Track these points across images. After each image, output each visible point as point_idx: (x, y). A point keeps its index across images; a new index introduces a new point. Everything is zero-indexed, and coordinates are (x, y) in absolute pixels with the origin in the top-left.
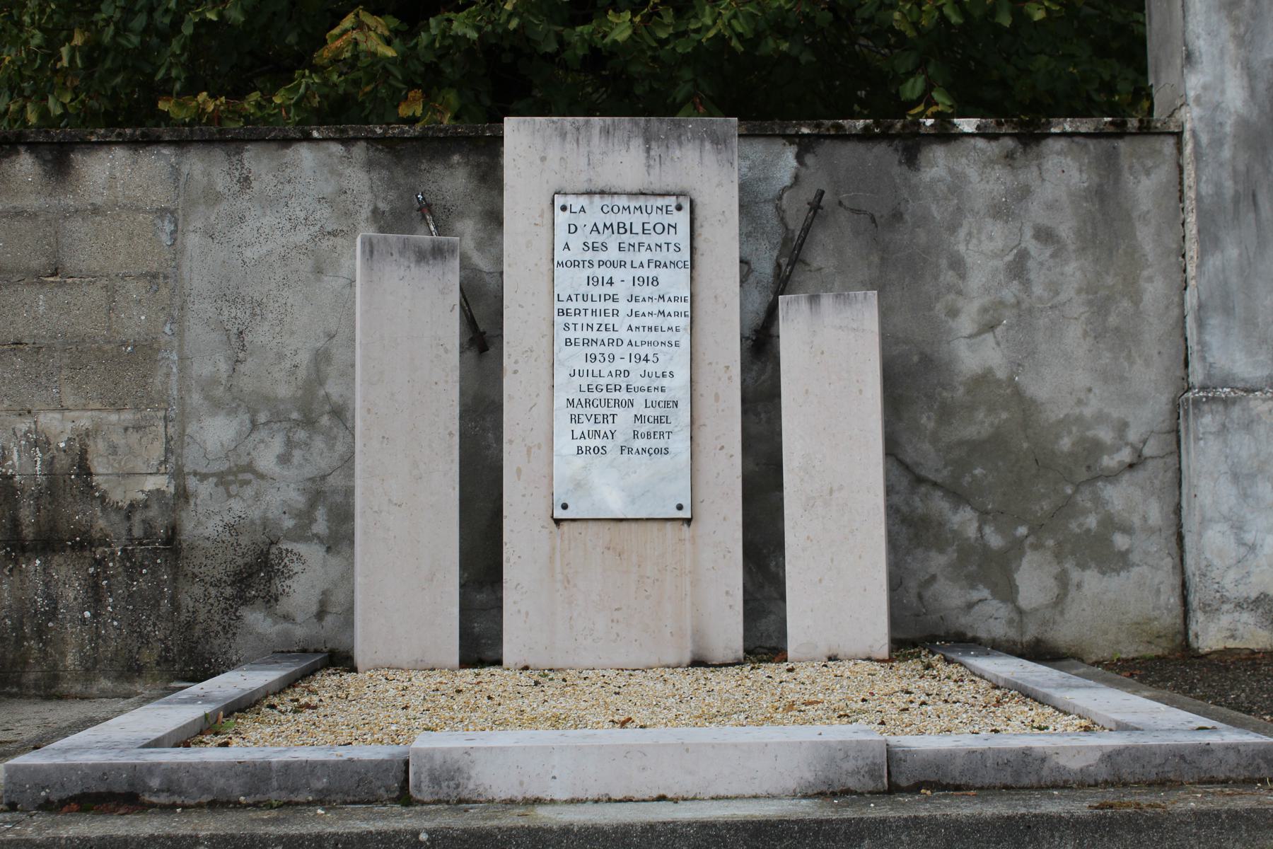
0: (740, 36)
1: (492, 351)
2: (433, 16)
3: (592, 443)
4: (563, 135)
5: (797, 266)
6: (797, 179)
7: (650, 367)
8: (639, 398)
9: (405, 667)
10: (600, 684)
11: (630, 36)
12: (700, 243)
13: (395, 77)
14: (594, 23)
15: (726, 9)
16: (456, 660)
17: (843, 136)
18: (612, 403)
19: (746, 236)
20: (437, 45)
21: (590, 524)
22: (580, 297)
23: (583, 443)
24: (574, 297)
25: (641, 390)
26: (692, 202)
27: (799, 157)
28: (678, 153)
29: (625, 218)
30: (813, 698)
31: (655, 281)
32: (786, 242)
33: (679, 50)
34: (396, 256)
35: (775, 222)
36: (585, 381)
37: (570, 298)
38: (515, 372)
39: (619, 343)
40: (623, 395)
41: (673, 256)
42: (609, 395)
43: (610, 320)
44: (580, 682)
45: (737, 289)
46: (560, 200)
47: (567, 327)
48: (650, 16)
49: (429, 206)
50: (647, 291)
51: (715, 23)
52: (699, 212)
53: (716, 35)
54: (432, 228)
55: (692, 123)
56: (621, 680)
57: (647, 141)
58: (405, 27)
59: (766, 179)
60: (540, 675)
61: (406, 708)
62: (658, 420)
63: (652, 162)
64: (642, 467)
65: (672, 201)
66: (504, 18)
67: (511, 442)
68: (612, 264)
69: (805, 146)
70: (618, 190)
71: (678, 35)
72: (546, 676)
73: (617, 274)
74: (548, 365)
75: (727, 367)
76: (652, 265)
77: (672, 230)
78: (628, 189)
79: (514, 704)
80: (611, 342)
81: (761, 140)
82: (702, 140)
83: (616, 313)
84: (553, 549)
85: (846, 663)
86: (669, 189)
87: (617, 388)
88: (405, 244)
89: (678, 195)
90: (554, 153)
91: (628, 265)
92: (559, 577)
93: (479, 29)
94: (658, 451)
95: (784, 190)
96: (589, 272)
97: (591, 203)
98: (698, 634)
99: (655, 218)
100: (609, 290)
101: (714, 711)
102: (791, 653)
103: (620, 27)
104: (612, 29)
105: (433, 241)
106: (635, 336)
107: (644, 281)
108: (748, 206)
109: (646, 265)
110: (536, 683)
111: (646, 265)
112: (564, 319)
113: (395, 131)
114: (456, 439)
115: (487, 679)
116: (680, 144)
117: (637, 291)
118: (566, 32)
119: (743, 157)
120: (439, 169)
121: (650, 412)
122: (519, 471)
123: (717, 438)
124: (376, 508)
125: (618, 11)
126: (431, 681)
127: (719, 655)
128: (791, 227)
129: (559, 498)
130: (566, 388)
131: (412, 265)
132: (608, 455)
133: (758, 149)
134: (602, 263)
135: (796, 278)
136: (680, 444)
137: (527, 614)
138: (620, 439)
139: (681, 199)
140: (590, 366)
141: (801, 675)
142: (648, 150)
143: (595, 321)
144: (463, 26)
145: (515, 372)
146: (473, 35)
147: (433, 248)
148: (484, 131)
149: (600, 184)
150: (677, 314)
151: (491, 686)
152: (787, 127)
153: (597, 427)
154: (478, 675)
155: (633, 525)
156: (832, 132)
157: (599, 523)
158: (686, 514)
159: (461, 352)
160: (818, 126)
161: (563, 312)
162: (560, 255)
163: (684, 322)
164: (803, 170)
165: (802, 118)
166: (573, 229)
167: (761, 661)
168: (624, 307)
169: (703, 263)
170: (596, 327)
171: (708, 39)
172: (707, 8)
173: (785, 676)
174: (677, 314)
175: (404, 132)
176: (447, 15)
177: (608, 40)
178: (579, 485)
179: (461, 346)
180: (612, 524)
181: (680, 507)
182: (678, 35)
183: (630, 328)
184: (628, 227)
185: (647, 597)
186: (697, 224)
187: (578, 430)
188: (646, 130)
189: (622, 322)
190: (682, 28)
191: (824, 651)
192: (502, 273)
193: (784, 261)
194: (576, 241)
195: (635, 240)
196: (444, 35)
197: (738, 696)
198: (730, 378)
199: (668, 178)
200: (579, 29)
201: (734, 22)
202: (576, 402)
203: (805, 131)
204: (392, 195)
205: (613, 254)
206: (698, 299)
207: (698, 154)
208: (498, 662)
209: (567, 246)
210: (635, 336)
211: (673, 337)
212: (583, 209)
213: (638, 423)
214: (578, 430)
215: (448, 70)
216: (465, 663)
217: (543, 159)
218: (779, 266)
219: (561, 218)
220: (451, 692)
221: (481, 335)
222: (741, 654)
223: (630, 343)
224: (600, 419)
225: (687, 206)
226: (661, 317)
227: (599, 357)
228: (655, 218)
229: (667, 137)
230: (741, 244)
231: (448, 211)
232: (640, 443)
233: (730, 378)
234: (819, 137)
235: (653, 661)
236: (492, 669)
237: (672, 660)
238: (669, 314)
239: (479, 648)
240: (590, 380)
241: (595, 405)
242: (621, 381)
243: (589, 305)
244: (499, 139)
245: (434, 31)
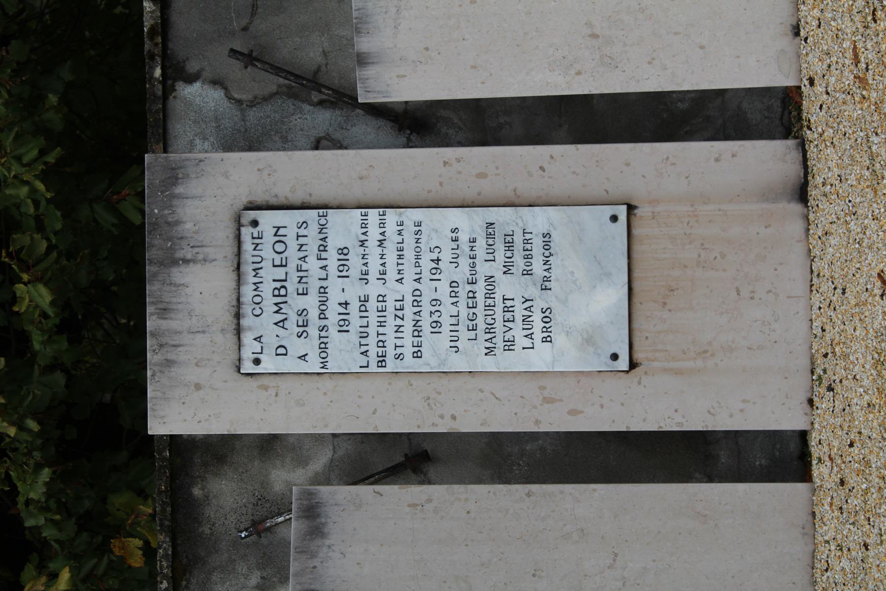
0: (43, 153)
1: (427, 446)
2: (21, 522)
4: (169, 363)
5: (322, 81)
6: (216, 82)
7: (446, 256)
8: (484, 269)
9: (811, 547)
10: (831, 313)
11: (46, 284)
12: (298, 197)
13: (95, 567)
14: (29, 328)
15: (9, 170)
16: (801, 487)
17: (164, 26)
18: (489, 301)
19: (286, 143)
20: (58, 517)
21: (635, 325)
22: (363, 341)
23: (538, 336)
24: (364, 349)
25: (473, 266)
27: (190, 79)
28: (189, 226)
29: (267, 289)
30: (849, 54)
31: (343, 251)
32: (292, 95)
33: (59, 226)
34: (316, 562)
35: (268, 108)
36: (464, 334)
37: (365, 353)
38: (454, 418)
40: (481, 288)
41: (313, 228)
43: (390, 305)
44: (828, 337)
45: (351, 152)
46: (248, 367)
47: (399, 357)
48: (20, 261)
49: (254, 524)
50: (355, 262)
51: (27, 183)
52: (260, 197)
53: (43, 181)
54: (281, 519)
55: (153, 209)
56: (826, 287)
57: (175, 262)
58: (35, 557)
59: (217, 119)
60: (819, 383)
61: (866, 546)
62: (509, 246)
63: (201, 257)
64: (568, 264)
65: (247, 232)
66: (25, 436)
67: (537, 422)
68: (323, 303)
69: (177, 73)
70: (234, 297)
71: (40, 227)
72: (820, 378)
73: (335, 297)
74: (445, 380)
75: (445, 163)
76: (324, 255)
78: (233, 284)
79: (860, 415)
80: (417, 303)
81: (170, 126)
82: (174, 196)
83: (382, 299)
84: (665, 370)
85: (802, 14)
86: (232, 236)
88: (301, 551)
89: (239, 226)
90: (192, 374)
92: (699, 363)
93: (39, 467)
94: (547, 246)
95: (230, 98)
96: (333, 332)
97: (250, 329)
98: (768, 195)
99: (267, 252)
100: (354, 306)
101: (867, 173)
102: (790, 82)
103: (35, 297)
104: (37, 306)
105: (298, 518)
106: (409, 274)
107: (343, 265)
108: (251, 142)
109: (324, 263)
110: (830, 389)
111: (324, 263)
112: (390, 359)
113: (164, 565)
114: (535, 488)
115: (826, 449)
116: (178, 223)
118: (42, 361)
119: (191, 147)
120: (210, 512)
122: (573, 412)
123: (530, 174)
124: (620, 584)
125: (14, 300)
126: (827, 516)
127: (791, 168)
128: (274, 88)
131: (327, 542)
132: (552, 305)
133: (182, 129)
134: (322, 316)
135: (336, 83)
136: (539, 220)
137: (744, 401)
138: (533, 291)
139: (244, 221)
140: (446, 328)
141: (818, 68)
142: (186, 261)
143: (391, 322)
144: (36, 486)
145: (454, 418)
146: (46, 474)
147: (307, 517)
148: (164, 459)
149: (228, 319)
150: (382, 225)
151: (836, 443)
152: (154, 95)
153: (519, 319)
154: (820, 460)
155: (636, 274)
156: (159, 40)
157: (634, 316)
159: (430, 483)
160: (152, 57)
161: (382, 362)
162: (314, 365)
163: (392, 216)
164: (205, 74)
165: (143, 77)
166: (282, 351)
167: (800, 118)
168: (374, 289)
169: (321, 192)
171: (48, 190)
172: (8, 192)
173: (819, 88)
174: (382, 225)
175: (166, 556)
176: (21, 506)
177: (50, 312)
178: (589, 340)
179: (422, 483)
180: (635, 300)
181: (614, 218)
182: (40, 227)
184: (278, 285)
185: (723, 256)
186: (273, 201)
187: (522, 341)
188: (161, 264)
190: (32, 223)
191: (786, 42)
192: (334, 435)
193: (315, 97)
194: (297, 346)
195: (294, 276)
196: (45, 509)
197: (846, 144)
199: (220, 236)
200: (37, 346)
201: (25, 160)
202: (488, 345)
203: (158, 72)
204: (242, 568)
205: (311, 302)
206: (364, 200)
207: (189, 202)
208: (803, 436)
209: (303, 357)
210: (409, 274)
211: (410, 228)
212: (258, 339)
214: (522, 341)
215: (87, 504)
216: (805, 476)
217: (198, 387)
218: (321, 103)
219: (269, 364)
220: (842, 493)
221: (408, 459)
222: (791, 143)
223: (418, 280)
224: (508, 315)
225: (253, 214)
226: (386, 244)
227: (435, 317)
228: (267, 252)
229: (170, 239)
230: (296, 148)
231: (260, 501)
232: (538, 267)
234: (166, 56)
235: (799, 249)
236: (813, 443)
237: (798, 227)
238: (383, 234)
239: (785, 458)
240: (462, 328)
241: (491, 321)
242: (463, 290)
243: (372, 330)
244: (174, 440)
245: (41, 521)
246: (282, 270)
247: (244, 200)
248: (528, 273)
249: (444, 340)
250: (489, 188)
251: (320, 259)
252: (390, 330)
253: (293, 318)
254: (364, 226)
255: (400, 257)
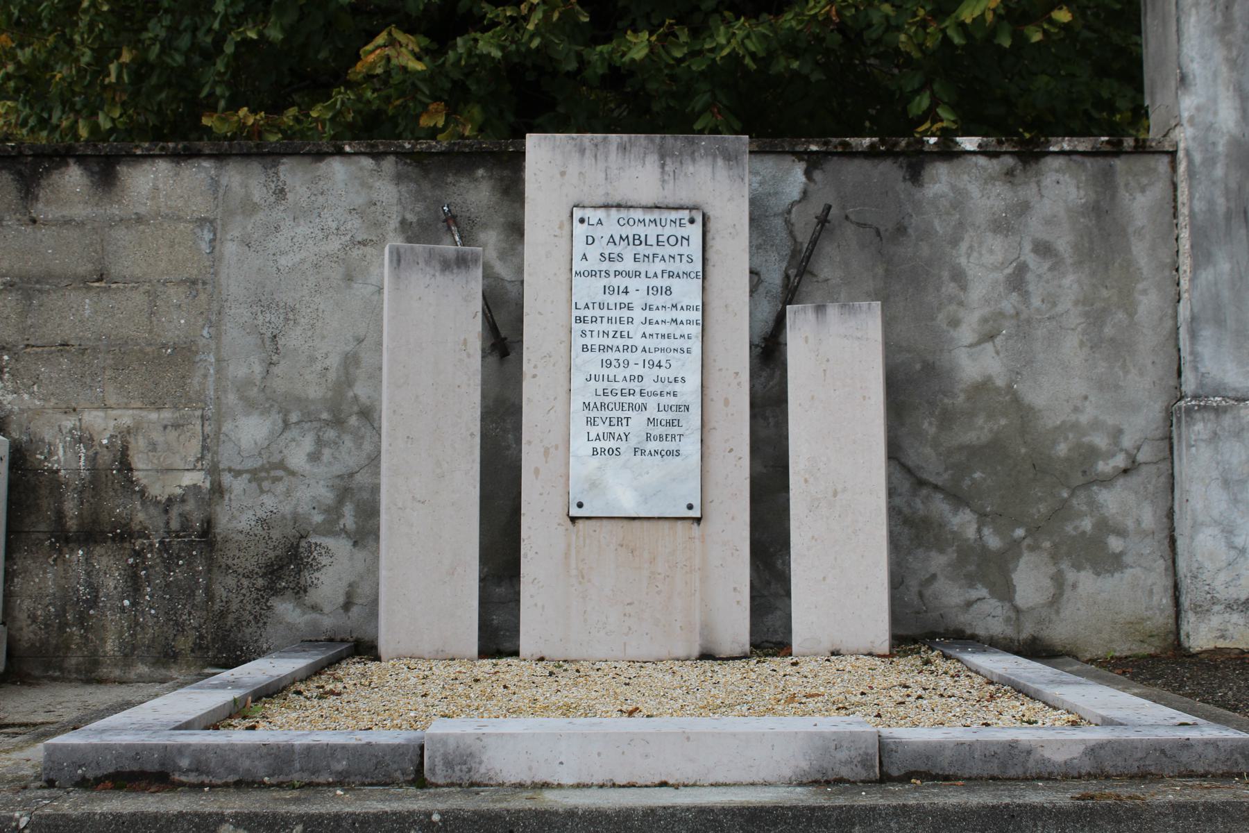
0: (753, 55)
1: (512, 356)
2: (461, 35)
3: (607, 444)
4: (582, 151)
5: (805, 277)
6: (805, 193)
7: (663, 373)
8: (652, 402)
9: (427, 656)
10: (611, 675)
11: (647, 56)
12: (711, 254)
13: (424, 93)
14: (614, 44)
15: (739, 29)
16: (475, 650)
17: (849, 153)
18: (626, 406)
19: (756, 248)
20: (463, 63)
21: (605, 522)
22: (596, 306)
23: (598, 445)
24: (591, 306)
25: (655, 394)
26: (704, 215)
27: (808, 173)
28: (691, 169)
29: (640, 230)
30: (814, 691)
31: (668, 291)
32: (794, 253)
33: (694, 68)
34: (422, 264)
35: (784, 234)
36: (600, 386)
37: (587, 306)
38: (534, 376)
39: (633, 349)
41: (686, 267)
42: (623, 399)
43: (625, 328)
44: (593, 673)
45: (747, 299)
46: (578, 214)
47: (584, 333)
48: (666, 35)
49: (454, 217)
50: (660, 300)
51: (729, 42)
52: (712, 226)
53: (729, 54)
54: (457, 238)
55: (705, 141)
56: (632, 672)
57: (662, 157)
58: (435, 46)
59: (776, 193)
60: (555, 666)
61: (425, 695)
62: (670, 423)
63: (666, 177)
65: (685, 214)
66: (526, 37)
68: (628, 274)
69: (813, 163)
70: (634, 204)
71: (693, 54)
72: (561, 666)
73: (632, 283)
74: (566, 370)
75: (737, 374)
76: (666, 275)
77: (685, 242)
78: (644, 203)
79: (529, 693)
81: (772, 157)
82: (715, 157)
83: (630, 321)
84: (569, 545)
85: (848, 658)
86: (682, 202)
88: (431, 253)
89: (690, 209)
90: (573, 168)
91: (643, 275)
92: (574, 572)
93: (502, 48)
94: (670, 453)
95: (793, 204)
96: (605, 281)
97: (608, 215)
98: (706, 629)
99: (669, 230)
101: (719, 702)
102: (795, 647)
103: (638, 46)
104: (630, 49)
105: (458, 252)
106: (649, 343)
108: (756, 220)
109: (659, 275)
110: (551, 674)
111: (659, 275)
112: (582, 326)
113: (422, 146)
114: (478, 440)
115: (504, 669)
116: (694, 160)
118: (586, 52)
119: (753, 172)
120: (464, 182)
121: (663, 416)
122: (537, 471)
123: (727, 441)
124: (400, 505)
125: (635, 31)
126: (451, 670)
127: (726, 649)
128: (800, 239)
129: (575, 497)
130: (582, 392)
131: (437, 274)
132: (622, 457)
133: (768, 165)
134: (618, 273)
135: (803, 289)
136: (690, 446)
137: (543, 607)
138: (633, 441)
139: (694, 213)
140: (605, 371)
141: (805, 668)
142: (663, 166)
143: (611, 328)
144: (488, 46)
145: (534, 376)
146: (497, 54)
147: (457, 258)
148: (507, 147)
149: (617, 198)
150: (689, 322)
151: (508, 676)
152: (797, 144)
153: (612, 430)
154: (496, 665)
155: (646, 524)
156: (840, 150)
157: (613, 521)
158: (696, 513)
159: (483, 357)
160: (826, 144)
161: (580, 320)
164: (812, 185)
165: (811, 136)
166: (590, 240)
167: (766, 655)
168: (638, 315)
171: (722, 58)
172: (722, 28)
173: (789, 670)
174: (689, 322)
175: (430, 147)
176: (473, 35)
177: (626, 59)
178: (594, 485)
179: (483, 350)
180: (625, 523)
182: (693, 54)
183: (644, 335)
184: (643, 239)
185: (659, 593)
186: (709, 236)
187: (594, 431)
188: (661, 146)
189: (636, 330)
190: (698, 48)
191: (827, 646)
192: (522, 282)
193: (792, 272)
194: (593, 252)
195: (649, 251)
196: (470, 53)
197: (743, 688)
198: (739, 384)
199: (683, 194)
200: (599, 48)
201: (747, 42)
203: (814, 148)
204: (419, 207)
205: (628, 264)
206: (709, 308)
207: (710, 169)
208: (515, 653)
209: (585, 257)
210: (649, 343)
211: (685, 344)
212: (600, 222)
214: (594, 431)
215: (473, 88)
216: (484, 653)
217: (563, 174)
218: (787, 277)
219: (579, 230)
220: (469, 681)
221: (502, 340)
222: (747, 648)
223: (644, 350)
224: (615, 421)
225: (699, 219)
227: (614, 363)
228: (669, 230)
229: (681, 154)
230: (751, 256)
231: (472, 222)
232: (652, 445)
233: (739, 384)
234: (826, 155)
235: (663, 653)
236: (509, 660)
237: (681, 653)
238: (682, 322)
239: (498, 639)
240: (605, 384)
241: (610, 408)
242: (635, 386)
243: (605, 313)
244: (521, 155)
245: (460, 50)
246: (654, 242)
247: (711, 213)
248: (648, 437)
249: (596, 370)
250: (716, 407)
251: (663, 272)
252: (605, 326)
253: (616, 250)
254: (688, 308)
255: (663, 336)
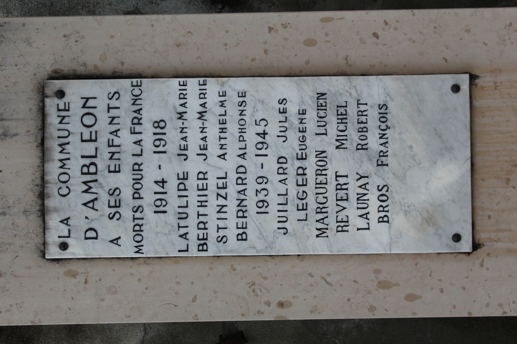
3: (374, 203)
7: (273, 129)
8: (314, 143)
12: (109, 66)
18: (321, 178)
22: (182, 223)
23: (374, 215)
24: (183, 231)
25: (303, 140)
26: (52, 78)
29: (75, 166)
36: (293, 215)
37: (184, 236)
39: (241, 171)
40: (311, 165)
41: (126, 99)
42: (311, 183)
43: (212, 182)
46: (54, 252)
47: (222, 240)
50: (172, 135)
52: (66, 66)
62: (342, 118)
64: (407, 137)
65: (51, 104)
67: (372, 309)
68: (137, 181)
70: (38, 175)
73: (150, 174)
74: (271, 264)
75: (270, 29)
76: (138, 128)
77: (91, 103)
78: (37, 162)
80: (241, 181)
83: (202, 176)
84: (510, 251)
86: (35, 108)
87: (302, 172)
89: (43, 95)
91: (139, 160)
94: (383, 117)
96: (149, 213)
97: (56, 210)
99: (75, 126)
100: (172, 185)
106: (233, 149)
107: (159, 139)
109: (138, 137)
111: (138, 137)
117: (172, 147)
121: (333, 129)
122: (411, 298)
123: (363, 41)
129: (444, 245)
130: (303, 239)
132: (389, 182)
134: (137, 195)
136: (374, 90)
138: (368, 168)
139: (49, 91)
140: (273, 208)
143: (213, 202)
149: (30, 199)
150: (202, 95)
153: (353, 197)
158: (464, 80)
161: (203, 245)
162: (127, 249)
163: (213, 86)
166: (92, 234)
169: (134, 61)
170: (221, 201)
174: (202, 95)
178: (429, 220)
181: (456, 88)
183: (222, 156)
184: (87, 161)
186: (81, 70)
187: (357, 222)
189: (215, 168)
195: (105, 152)
198: (285, 26)
202: (320, 226)
205: (124, 180)
209: (115, 241)
210: (233, 149)
211: (233, 99)
212: (65, 221)
213: (347, 144)
214: (357, 222)
219: (77, 249)
223: (242, 156)
224: (342, 193)
225: (58, 84)
226: (206, 116)
227: (261, 197)
228: (75, 126)
232: (373, 141)
233: (285, 26)
238: (203, 105)
240: (291, 207)
241: (323, 201)
242: (292, 166)
243: (192, 211)
246: (92, 145)
247: (49, 69)
248: (362, 148)
249: (271, 222)
250: (317, 56)
251: (133, 133)
252: (211, 210)
253: (104, 197)
254: (183, 96)
255: (223, 130)
